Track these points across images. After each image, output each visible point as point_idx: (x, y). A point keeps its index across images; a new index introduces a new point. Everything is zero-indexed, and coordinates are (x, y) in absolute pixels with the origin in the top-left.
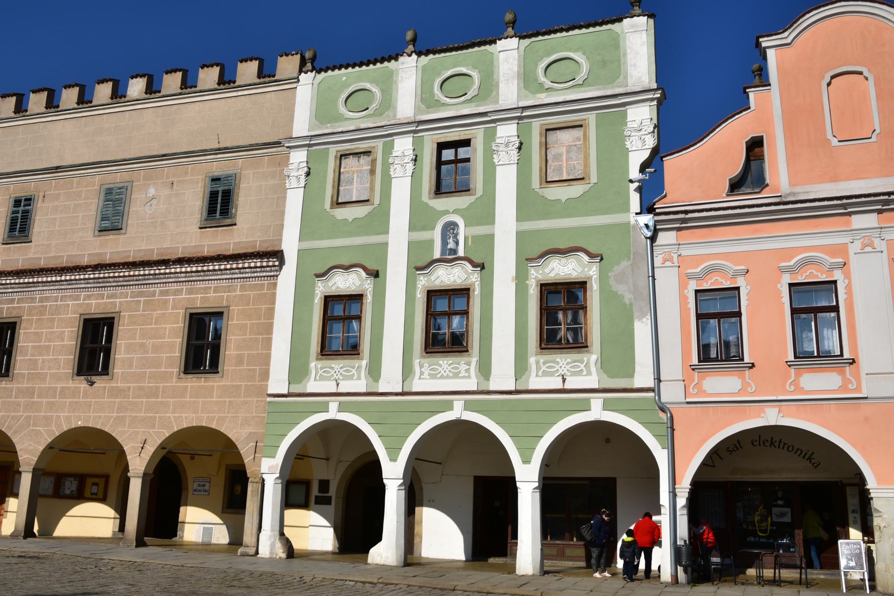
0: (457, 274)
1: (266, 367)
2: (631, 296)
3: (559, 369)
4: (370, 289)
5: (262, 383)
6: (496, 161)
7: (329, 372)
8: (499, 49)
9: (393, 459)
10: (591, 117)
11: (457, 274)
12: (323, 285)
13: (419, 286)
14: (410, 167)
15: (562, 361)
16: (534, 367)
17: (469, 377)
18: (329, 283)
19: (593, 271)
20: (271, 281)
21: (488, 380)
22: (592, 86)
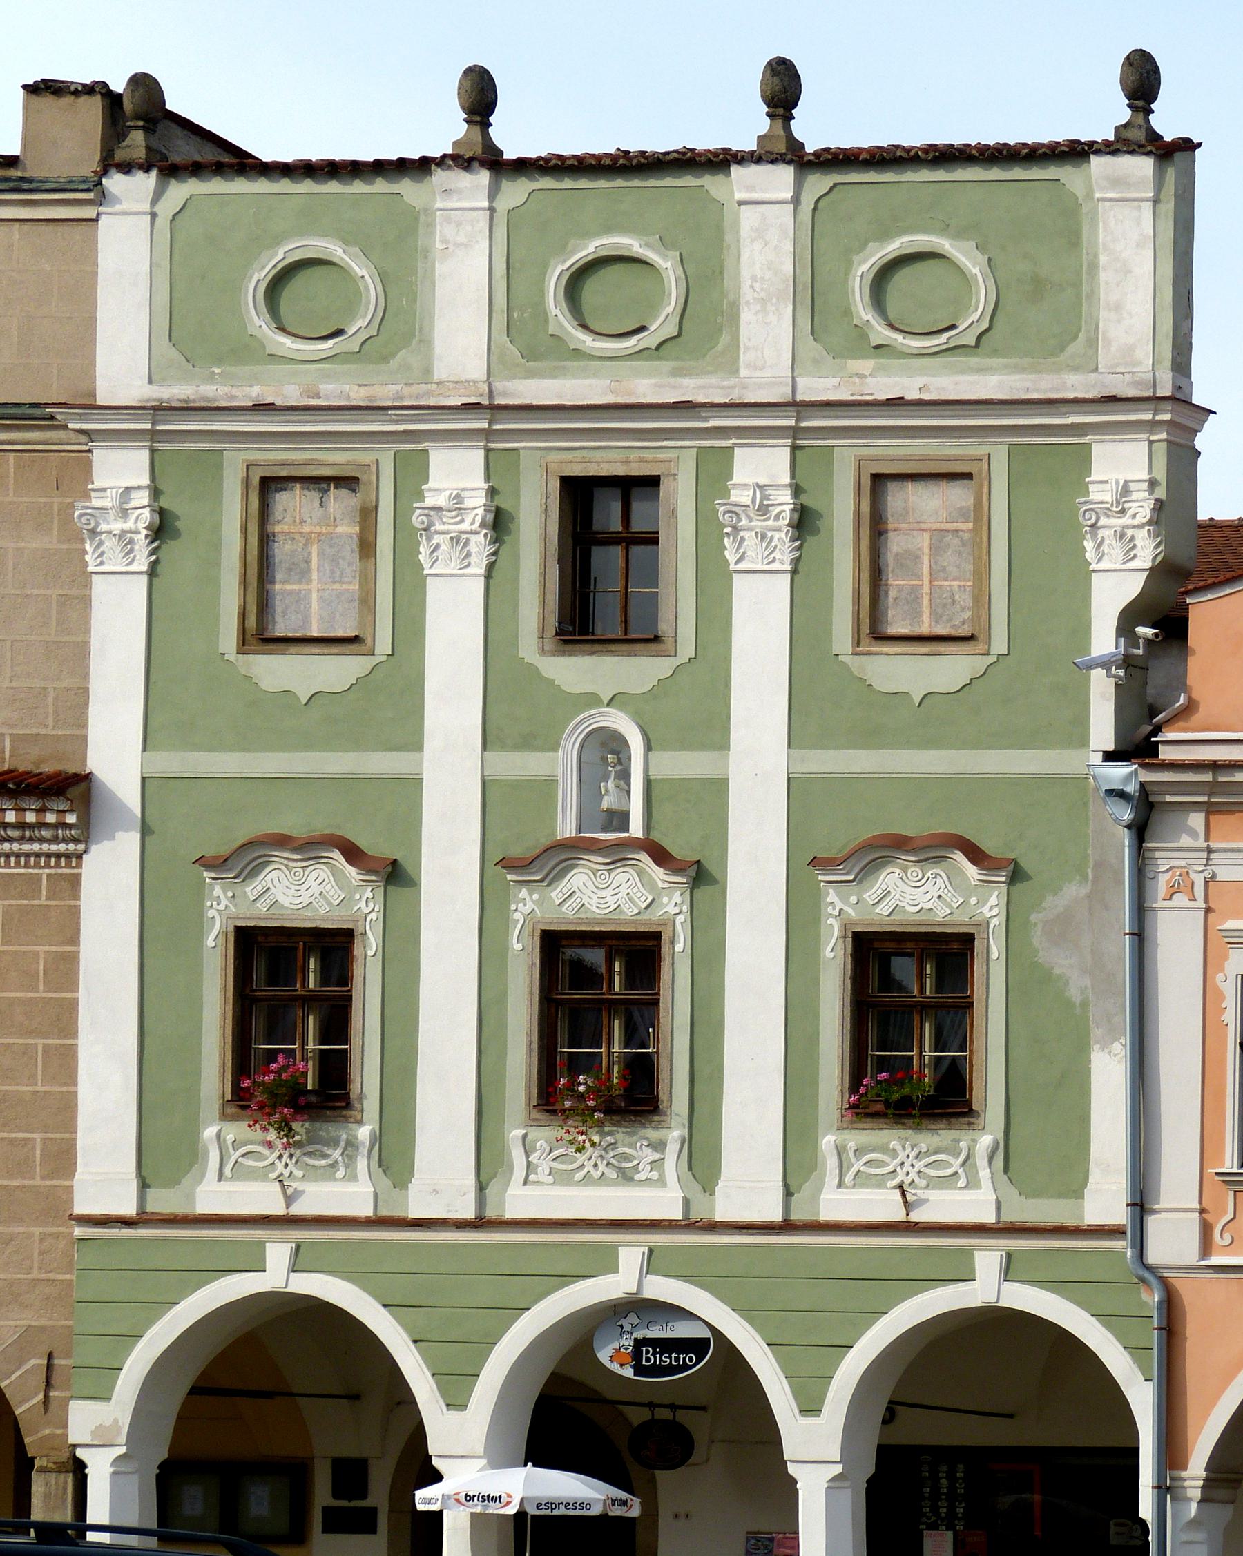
0: (623, 891)
1: (67, 1135)
2: (1087, 982)
3: (899, 1169)
4: (373, 916)
5: (55, 1182)
6: (730, 556)
7: (261, 1157)
8: (739, 196)
9: (456, 1402)
10: (998, 451)
11: (623, 891)
12: (230, 894)
13: (517, 915)
14: (480, 546)
15: (904, 1148)
16: (832, 1162)
17: (661, 1182)
18: (248, 890)
19: (991, 908)
20: (60, 871)
21: (712, 1194)
22: (1004, 357)
